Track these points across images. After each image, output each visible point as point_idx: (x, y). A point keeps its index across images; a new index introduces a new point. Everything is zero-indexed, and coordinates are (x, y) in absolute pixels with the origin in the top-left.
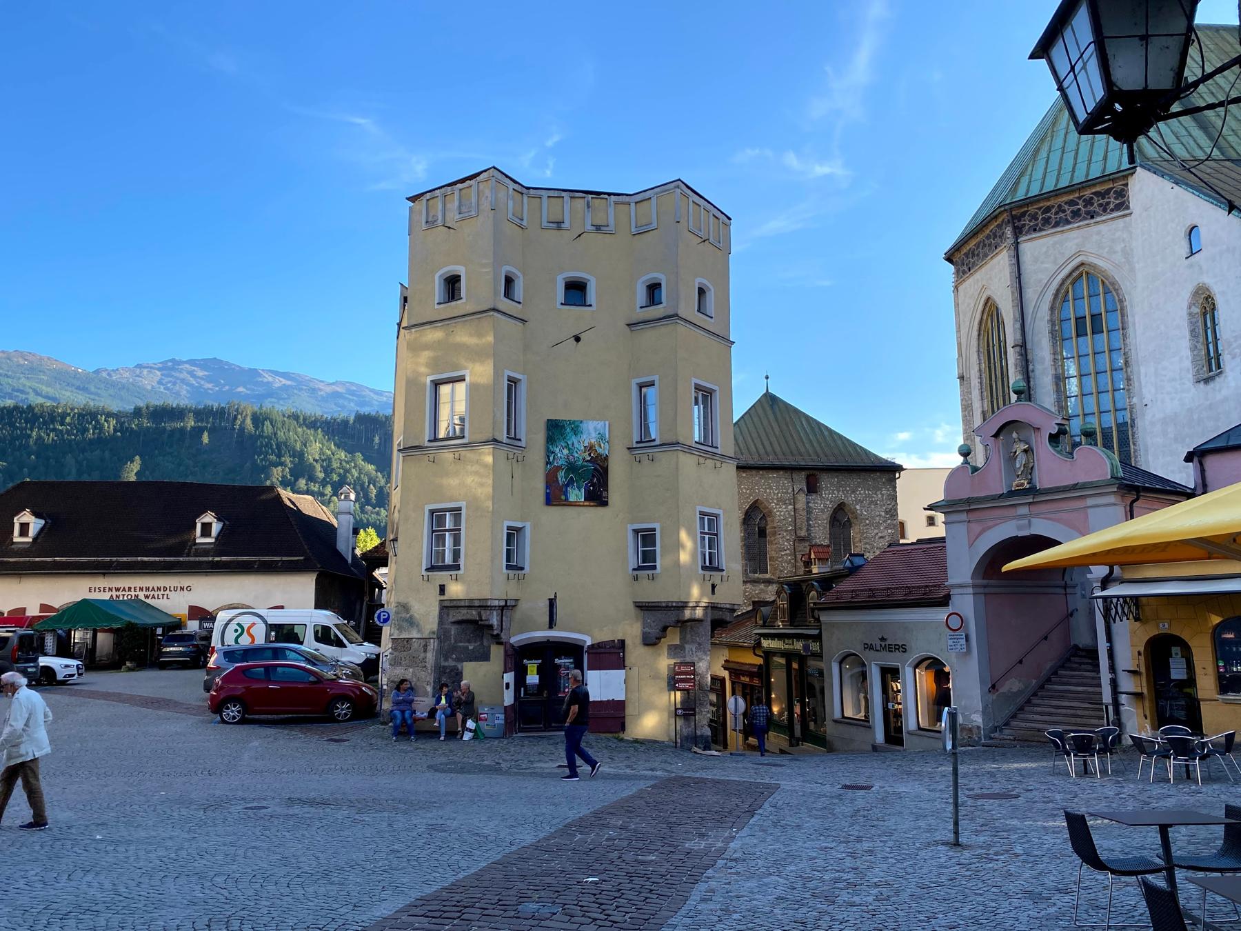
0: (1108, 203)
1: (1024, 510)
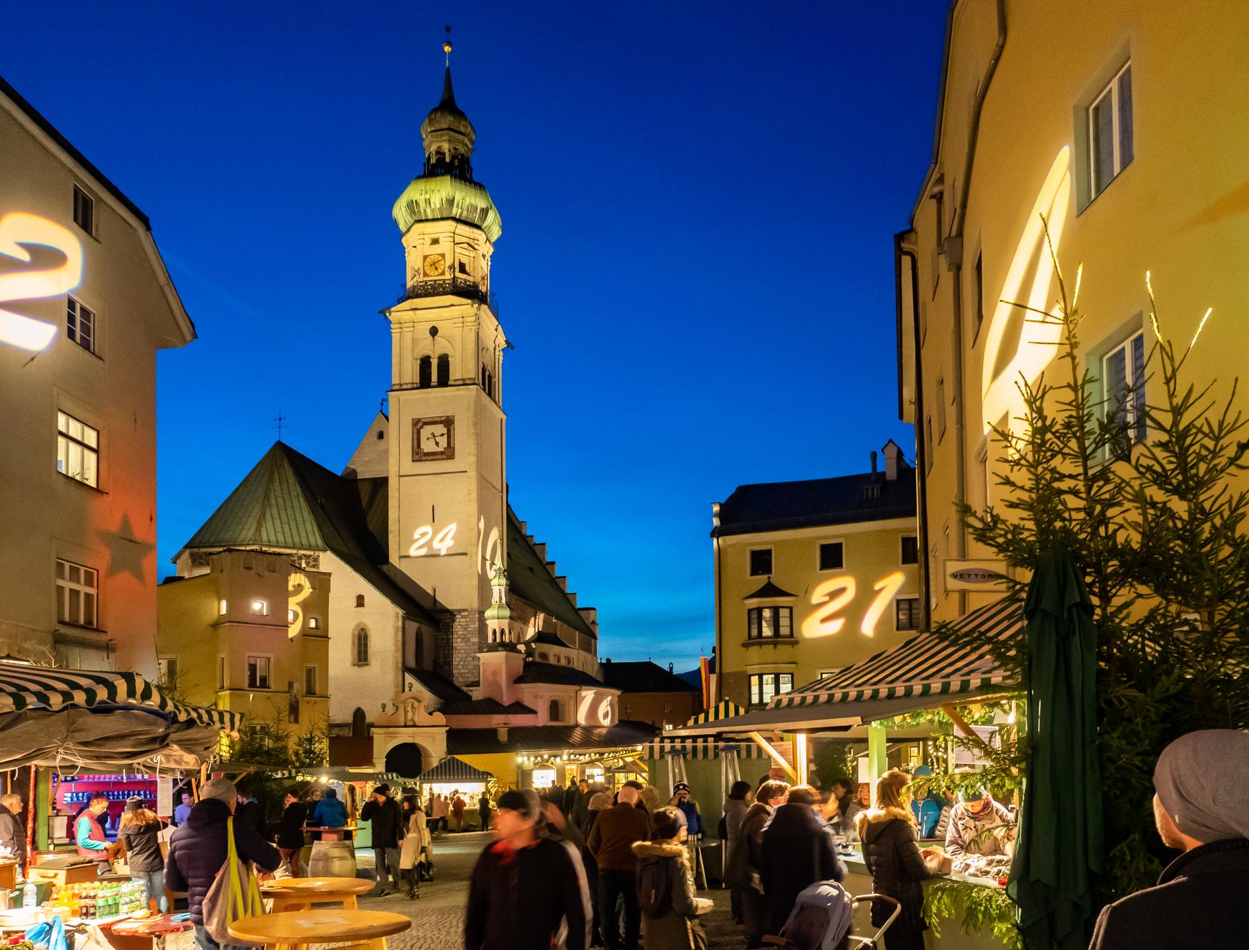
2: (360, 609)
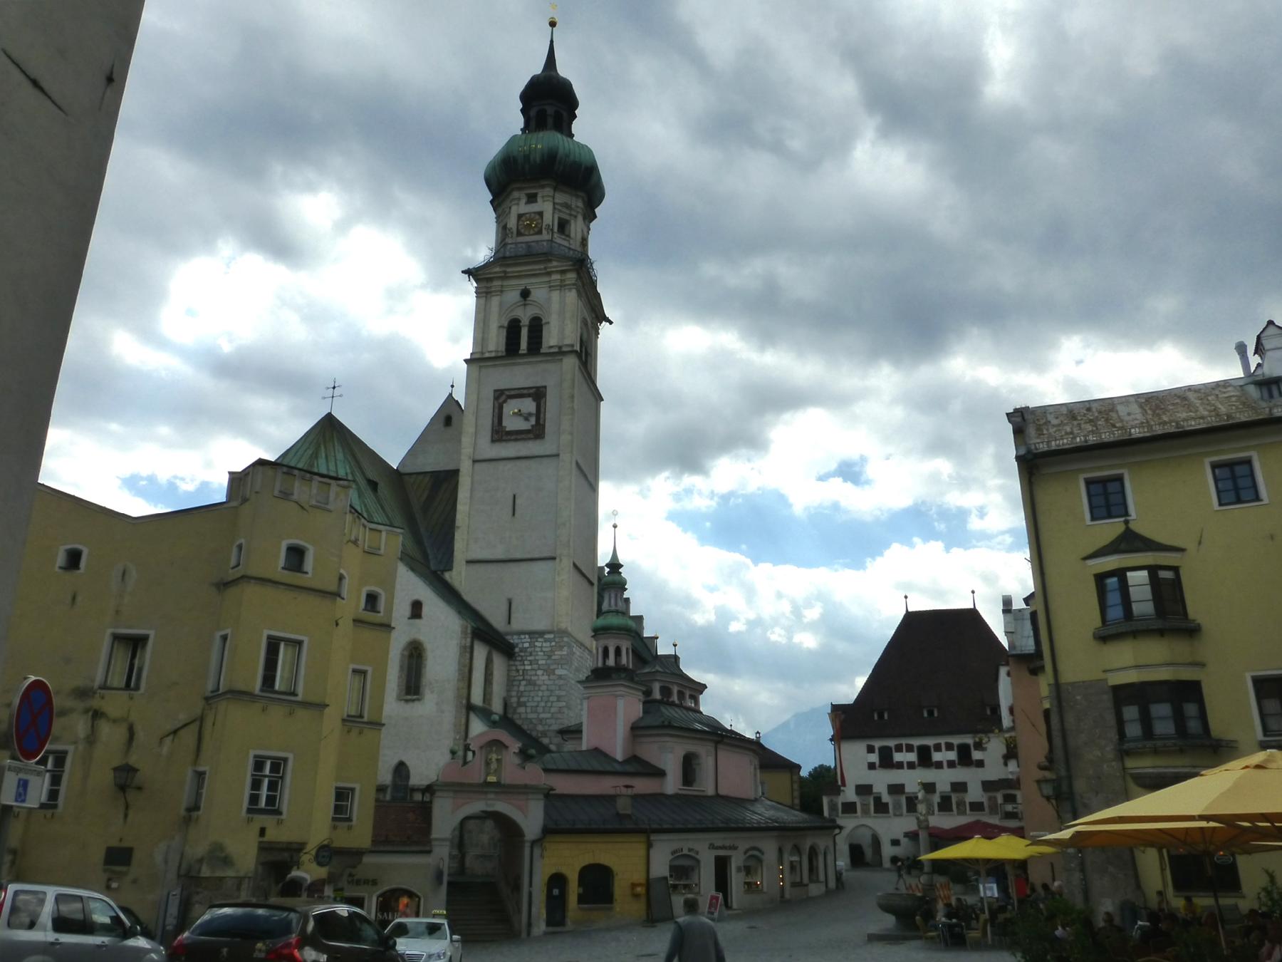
2: (417, 621)
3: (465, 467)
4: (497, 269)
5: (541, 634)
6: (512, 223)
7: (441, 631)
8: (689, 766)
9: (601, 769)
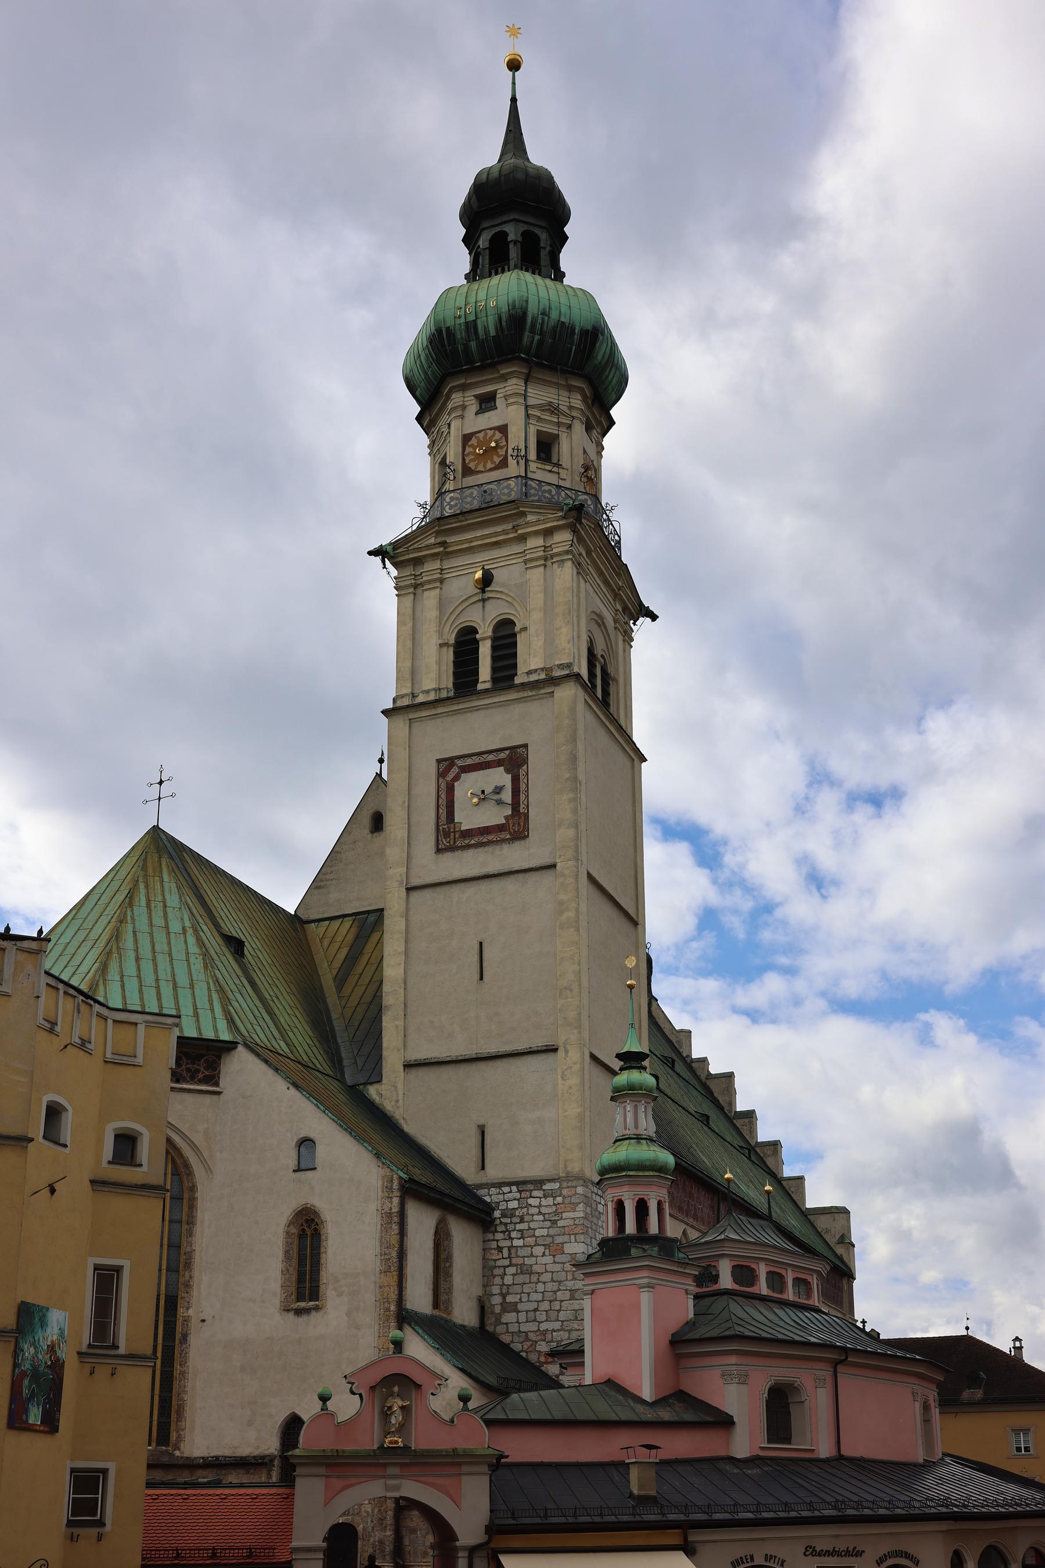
0: (197, 1071)
1: (396, 1471)
3: (394, 902)
4: (432, 541)
5: (539, 1183)
6: (453, 452)
7: (352, 1186)
8: (780, 1405)
9: (613, 1417)
